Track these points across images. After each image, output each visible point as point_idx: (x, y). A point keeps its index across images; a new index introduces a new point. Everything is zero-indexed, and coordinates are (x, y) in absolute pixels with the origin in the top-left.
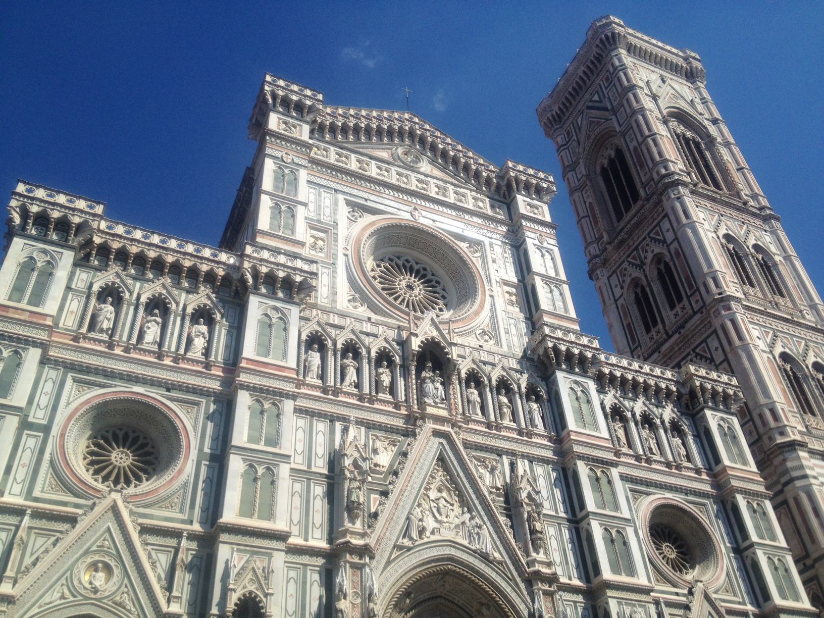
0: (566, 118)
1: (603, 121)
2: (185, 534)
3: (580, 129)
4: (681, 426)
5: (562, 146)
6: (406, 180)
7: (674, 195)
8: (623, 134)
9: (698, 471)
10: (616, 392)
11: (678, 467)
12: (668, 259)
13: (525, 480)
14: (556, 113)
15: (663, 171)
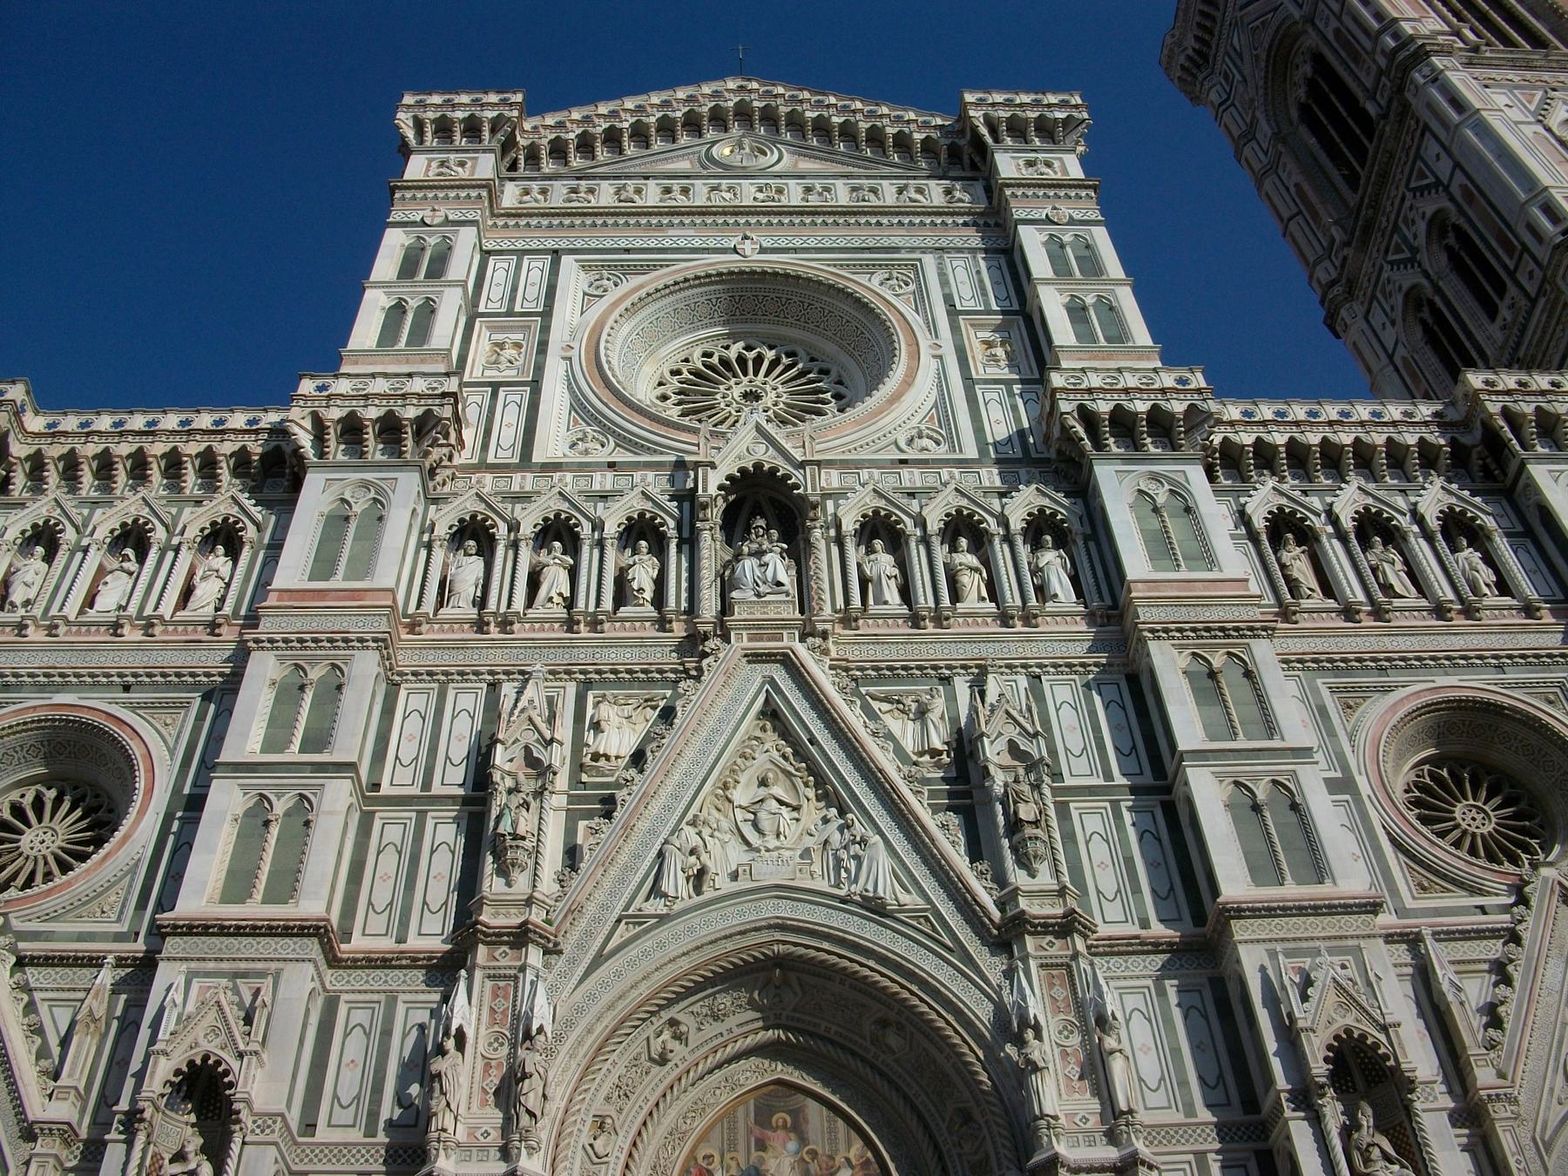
0: (1213, 51)
1: (1270, 15)
2: (110, 959)
3: (1240, 56)
4: (1474, 519)
5: (1220, 105)
6: (727, 196)
7: (1425, 77)
8: (1310, 20)
9: (1529, 610)
10: (1282, 480)
11: (1469, 611)
12: (1455, 217)
13: (1000, 714)
14: (1194, 50)
15: (1392, 44)
